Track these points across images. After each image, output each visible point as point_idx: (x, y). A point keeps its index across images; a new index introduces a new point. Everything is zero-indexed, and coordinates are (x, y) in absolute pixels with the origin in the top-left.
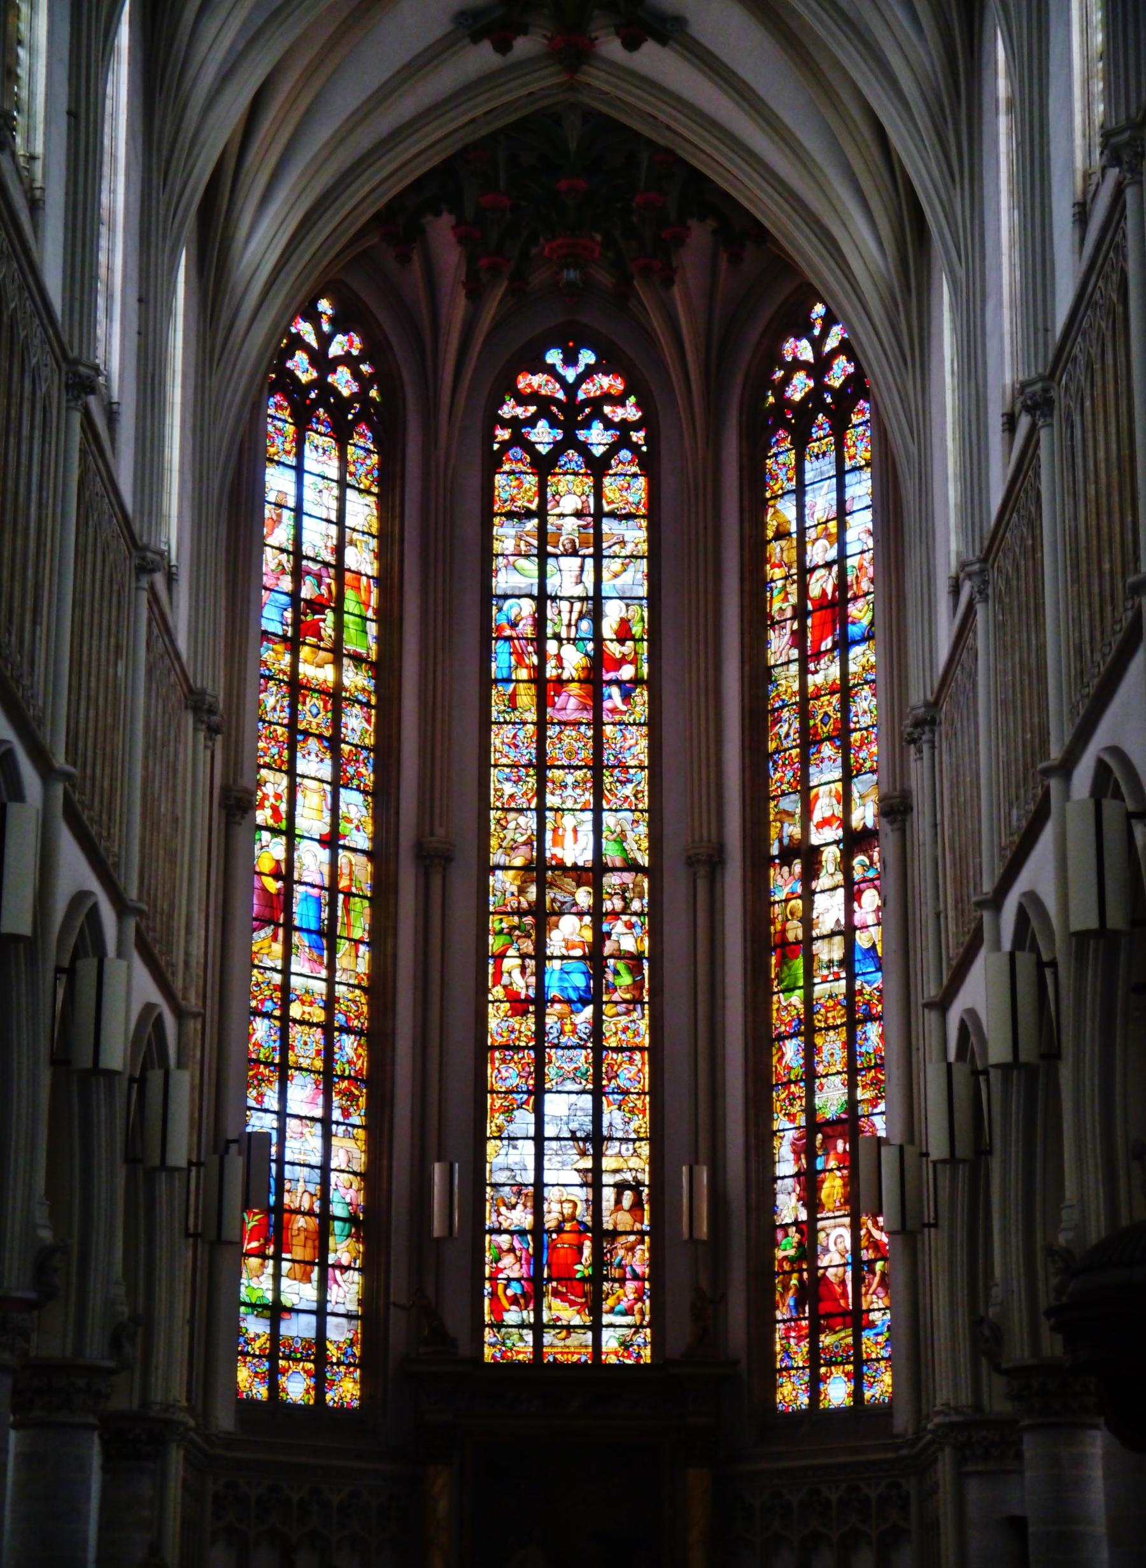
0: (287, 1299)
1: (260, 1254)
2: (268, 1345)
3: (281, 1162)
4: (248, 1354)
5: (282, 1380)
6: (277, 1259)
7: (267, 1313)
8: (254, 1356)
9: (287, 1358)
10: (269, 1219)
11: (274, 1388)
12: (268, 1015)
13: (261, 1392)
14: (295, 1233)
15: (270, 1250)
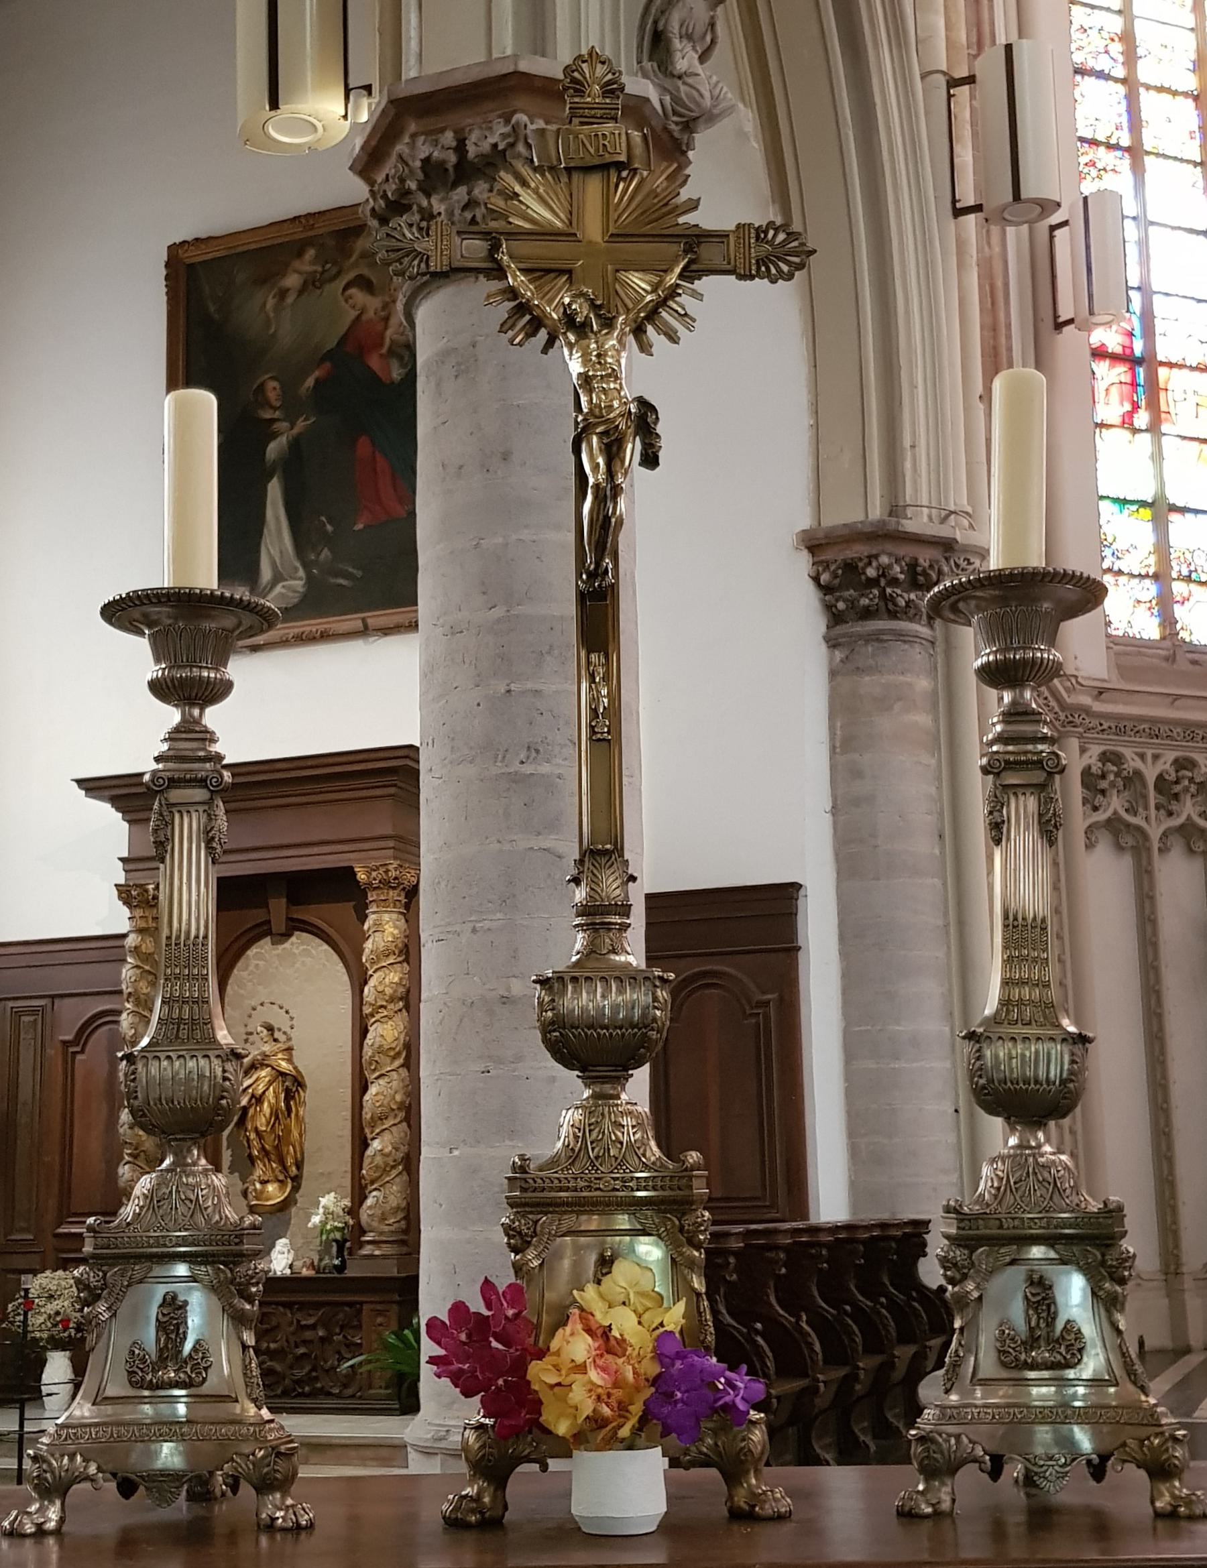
0: (1174, 498)
1: (1127, 422)
2: (1152, 560)
3: (1145, 289)
4: (1120, 572)
5: (1178, 611)
6: (1154, 428)
7: (1146, 513)
8: (1132, 576)
9: (1188, 579)
10: (1134, 376)
11: (1168, 621)
12: (1101, 75)
13: (1149, 628)
14: (1179, 396)
15: (1142, 419)
